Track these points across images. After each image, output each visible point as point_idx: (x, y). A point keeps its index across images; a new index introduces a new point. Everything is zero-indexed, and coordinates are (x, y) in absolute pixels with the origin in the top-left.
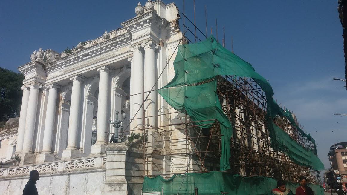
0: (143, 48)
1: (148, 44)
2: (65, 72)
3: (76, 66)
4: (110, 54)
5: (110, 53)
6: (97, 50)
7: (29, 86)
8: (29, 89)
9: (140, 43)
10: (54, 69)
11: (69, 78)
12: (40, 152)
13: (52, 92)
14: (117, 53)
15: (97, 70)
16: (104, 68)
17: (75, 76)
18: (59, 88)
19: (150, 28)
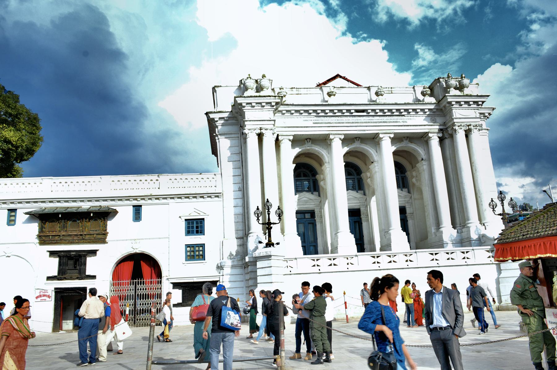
4: (398, 120)
7: (263, 131)
16: (392, 136)
17: (341, 134)
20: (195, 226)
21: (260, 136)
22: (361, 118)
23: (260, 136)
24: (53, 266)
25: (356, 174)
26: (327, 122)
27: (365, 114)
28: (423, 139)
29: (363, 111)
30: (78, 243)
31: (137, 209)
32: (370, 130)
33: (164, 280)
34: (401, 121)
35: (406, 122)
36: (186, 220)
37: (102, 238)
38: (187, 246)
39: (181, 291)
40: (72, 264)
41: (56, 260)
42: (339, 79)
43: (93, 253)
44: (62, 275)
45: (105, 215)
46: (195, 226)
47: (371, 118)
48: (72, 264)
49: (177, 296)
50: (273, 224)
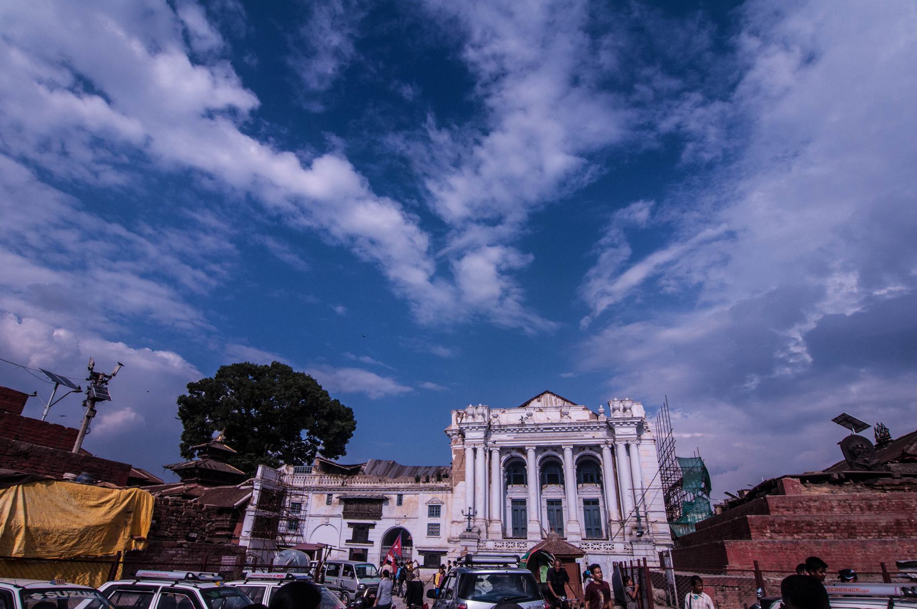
5: (578, 434)
12: (490, 521)
13: (496, 455)
14: (586, 436)
20: (434, 510)
21: (475, 450)
23: (475, 450)
24: (349, 533)
25: (551, 472)
28: (597, 448)
30: (365, 519)
31: (400, 497)
33: (414, 548)
37: (378, 516)
38: (429, 525)
40: (360, 533)
41: (351, 530)
42: (548, 395)
43: (373, 526)
44: (355, 540)
45: (383, 500)
46: (434, 510)
48: (360, 533)
49: (421, 560)
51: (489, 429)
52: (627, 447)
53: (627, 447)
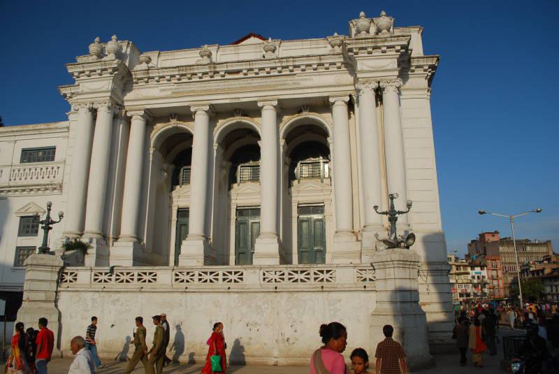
0: (384, 89)
1: (394, 84)
2: (176, 92)
3: (206, 88)
4: (286, 82)
6: (261, 69)
7: (95, 106)
8: (94, 112)
9: (379, 79)
10: (147, 82)
11: (189, 107)
12: (116, 239)
13: (137, 126)
15: (260, 104)
16: (275, 103)
18: (150, 119)
19: (396, 60)
21: (94, 112)
22: (236, 82)
26: (189, 90)
27: (241, 75)
28: (324, 105)
29: (238, 72)
32: (246, 98)
34: (291, 82)
35: (298, 84)
36: (22, 217)
38: (19, 249)
39: (5, 302)
47: (249, 81)
50: (53, 222)
51: (125, 80)
52: (379, 94)
53: (379, 94)
